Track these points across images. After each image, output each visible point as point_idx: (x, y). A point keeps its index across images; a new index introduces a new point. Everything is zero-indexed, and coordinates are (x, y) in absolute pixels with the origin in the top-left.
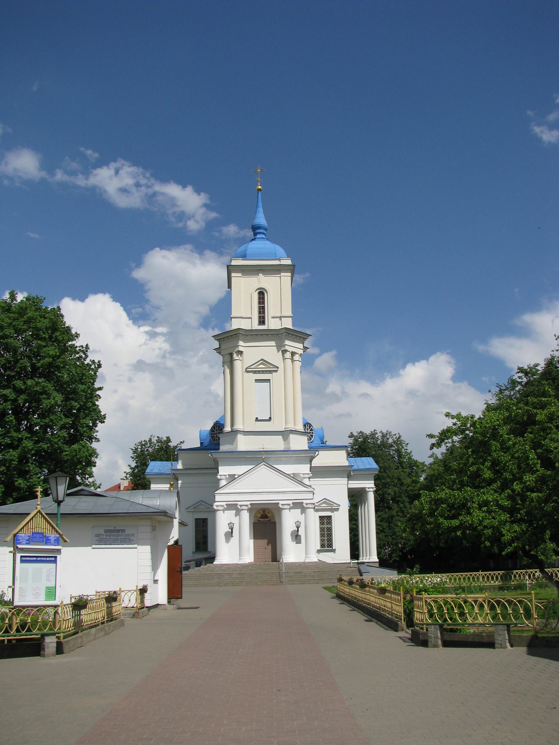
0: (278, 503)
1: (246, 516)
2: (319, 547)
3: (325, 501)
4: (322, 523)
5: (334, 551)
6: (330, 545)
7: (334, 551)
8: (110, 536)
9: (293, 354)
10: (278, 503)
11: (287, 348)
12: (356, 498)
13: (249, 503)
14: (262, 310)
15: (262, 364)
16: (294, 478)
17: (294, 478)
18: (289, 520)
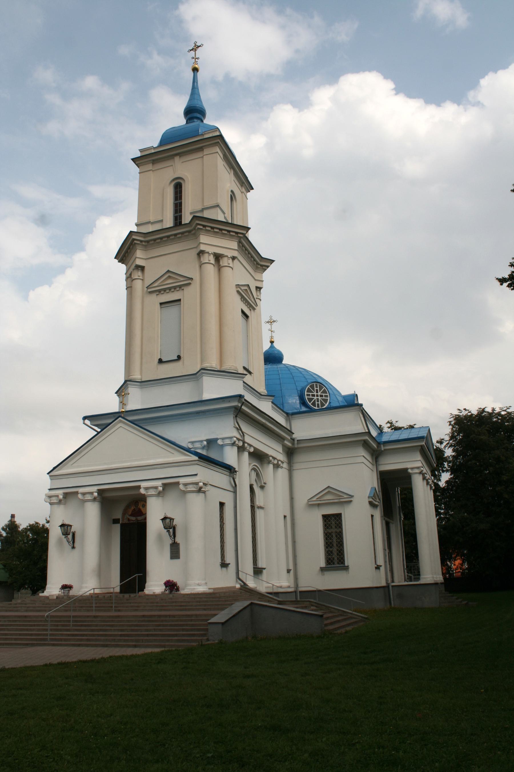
0: (139, 487)
1: (93, 511)
2: (323, 564)
3: (329, 490)
5: (346, 568)
6: (341, 559)
10: (139, 487)
11: (202, 247)
13: (95, 489)
15: (169, 277)
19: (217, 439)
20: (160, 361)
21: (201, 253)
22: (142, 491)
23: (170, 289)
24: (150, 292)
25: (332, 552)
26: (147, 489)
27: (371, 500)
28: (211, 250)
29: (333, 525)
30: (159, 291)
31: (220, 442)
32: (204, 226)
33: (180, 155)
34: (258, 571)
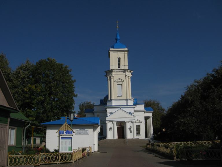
1: (115, 124)
3: (138, 120)
4: (137, 127)
7: (141, 135)
8: (81, 131)
12: (146, 118)
14: (119, 64)
16: (130, 113)
17: (130, 113)
18: (128, 125)
20: (118, 96)
28: (128, 75)
29: (138, 127)
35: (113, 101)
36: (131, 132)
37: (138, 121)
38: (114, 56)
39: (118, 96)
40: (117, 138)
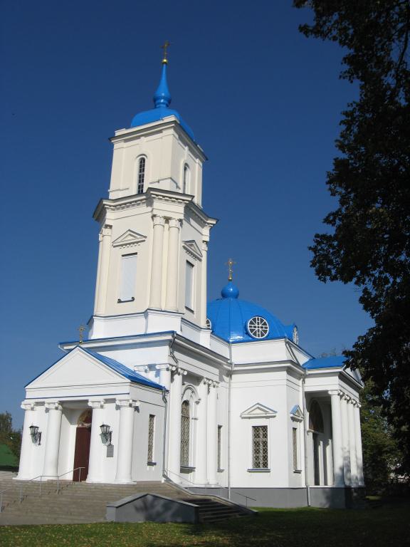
0: (87, 401)
2: (251, 467)
3: (260, 406)
4: (256, 435)
6: (265, 465)
7: (269, 471)
9: (167, 220)
10: (87, 401)
11: (155, 212)
19: (155, 365)
20: (120, 301)
21: (154, 216)
22: (90, 404)
23: (130, 244)
24: (114, 247)
25: (258, 457)
26: (93, 402)
27: (292, 415)
29: (260, 434)
30: (122, 245)
31: (157, 367)
32: (157, 195)
33: (146, 135)
34: (186, 469)
35: (98, 324)
36: (110, 453)
37: (258, 411)
38: (124, 156)
39: (120, 301)
40: (72, 479)
